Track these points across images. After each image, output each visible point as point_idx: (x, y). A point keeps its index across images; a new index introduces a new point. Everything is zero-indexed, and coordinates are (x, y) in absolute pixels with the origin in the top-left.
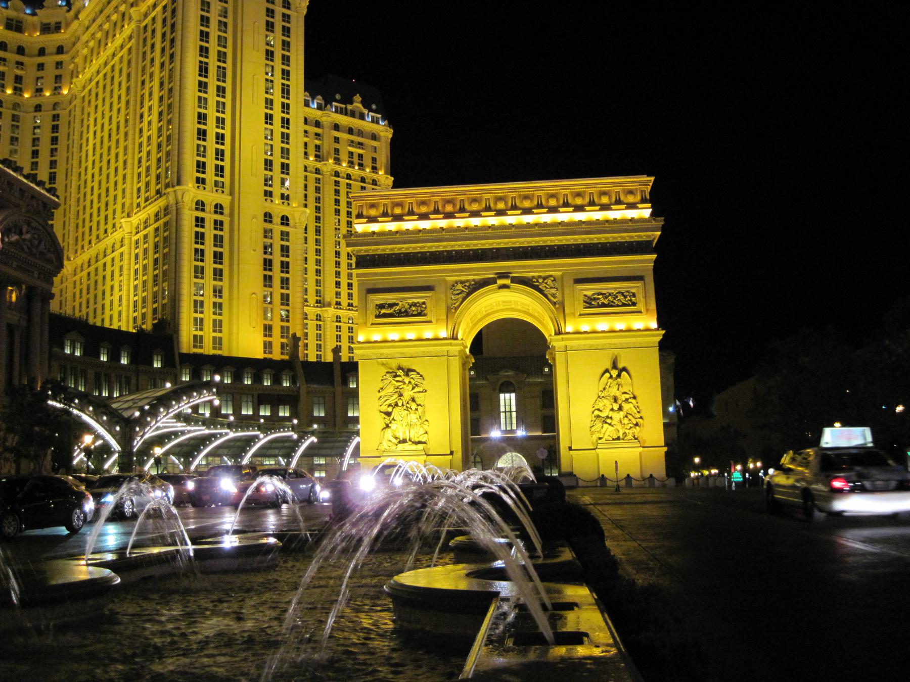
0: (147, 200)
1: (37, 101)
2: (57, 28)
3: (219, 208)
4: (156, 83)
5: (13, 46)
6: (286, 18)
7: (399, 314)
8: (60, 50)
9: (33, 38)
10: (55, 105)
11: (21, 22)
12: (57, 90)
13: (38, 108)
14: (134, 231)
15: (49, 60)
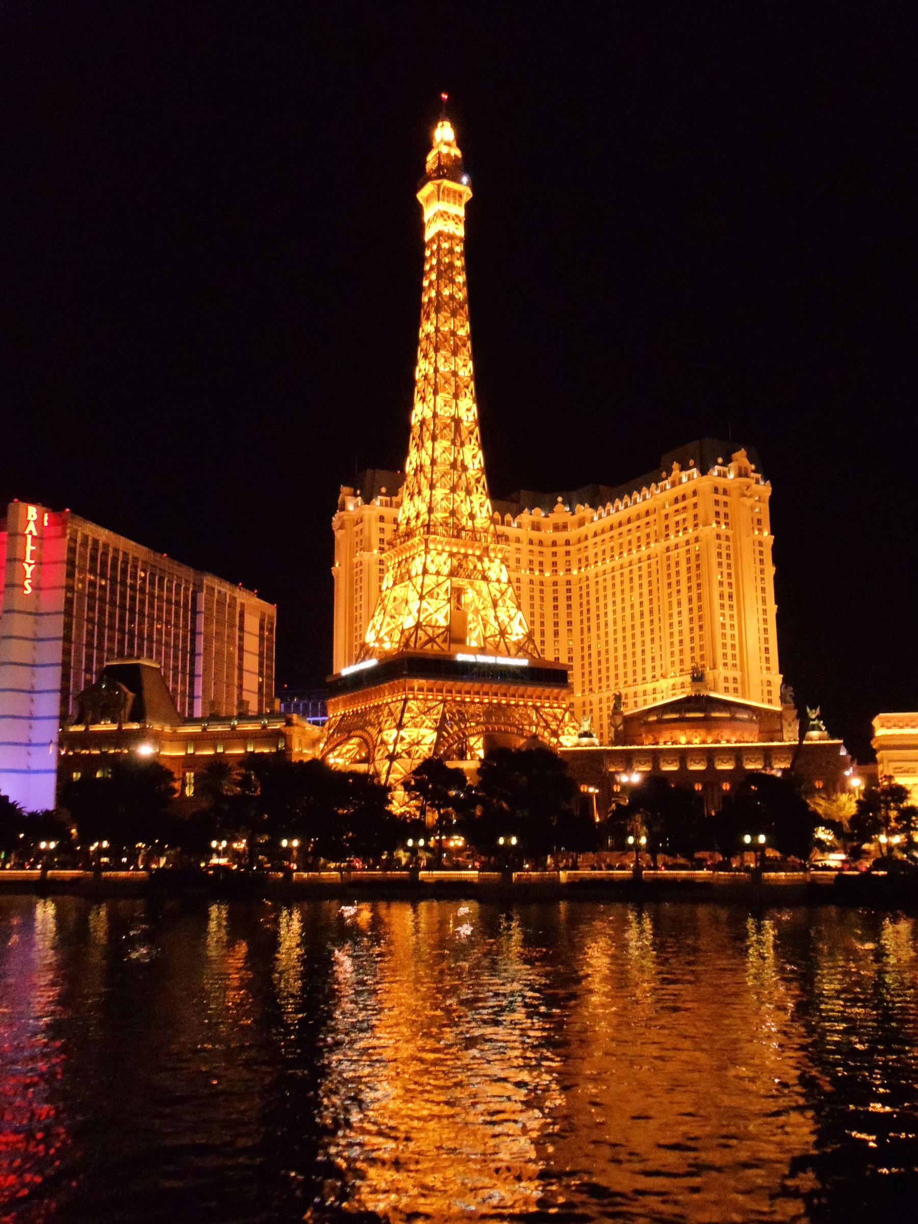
0: (682, 670)
1: (555, 578)
2: (565, 527)
3: (735, 679)
4: (684, 597)
5: (536, 541)
6: (761, 553)
7: (904, 772)
8: (567, 543)
9: (548, 534)
10: (568, 583)
11: (538, 523)
12: (569, 570)
13: (555, 584)
14: (670, 688)
15: (561, 550)
